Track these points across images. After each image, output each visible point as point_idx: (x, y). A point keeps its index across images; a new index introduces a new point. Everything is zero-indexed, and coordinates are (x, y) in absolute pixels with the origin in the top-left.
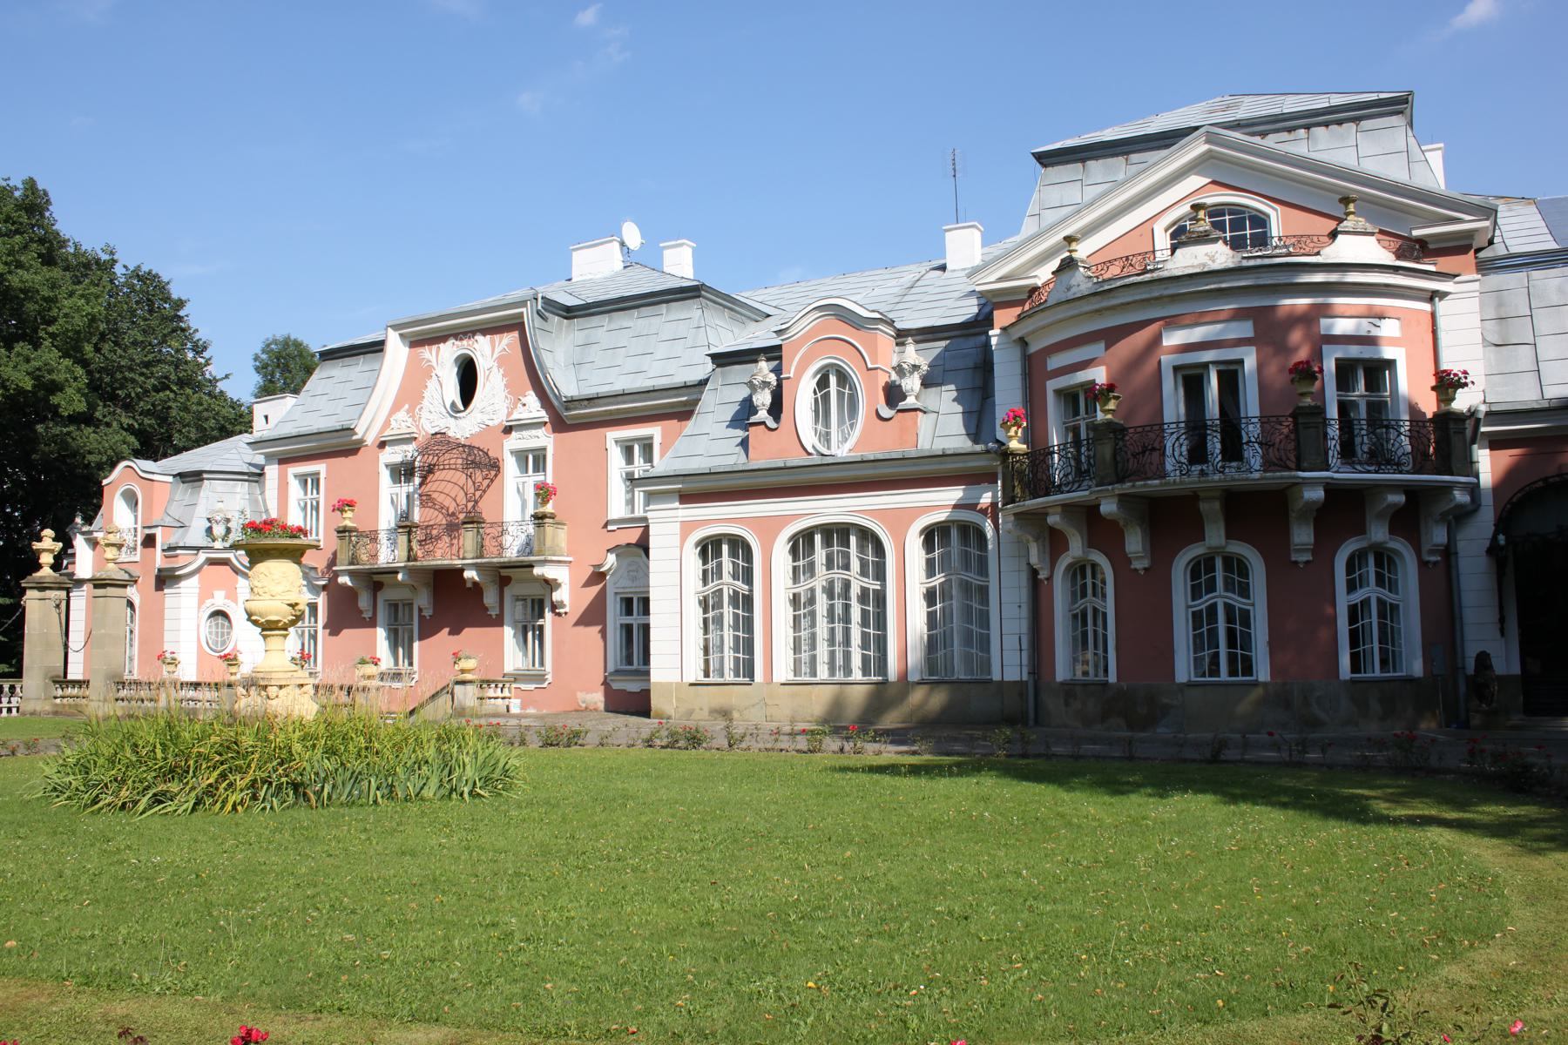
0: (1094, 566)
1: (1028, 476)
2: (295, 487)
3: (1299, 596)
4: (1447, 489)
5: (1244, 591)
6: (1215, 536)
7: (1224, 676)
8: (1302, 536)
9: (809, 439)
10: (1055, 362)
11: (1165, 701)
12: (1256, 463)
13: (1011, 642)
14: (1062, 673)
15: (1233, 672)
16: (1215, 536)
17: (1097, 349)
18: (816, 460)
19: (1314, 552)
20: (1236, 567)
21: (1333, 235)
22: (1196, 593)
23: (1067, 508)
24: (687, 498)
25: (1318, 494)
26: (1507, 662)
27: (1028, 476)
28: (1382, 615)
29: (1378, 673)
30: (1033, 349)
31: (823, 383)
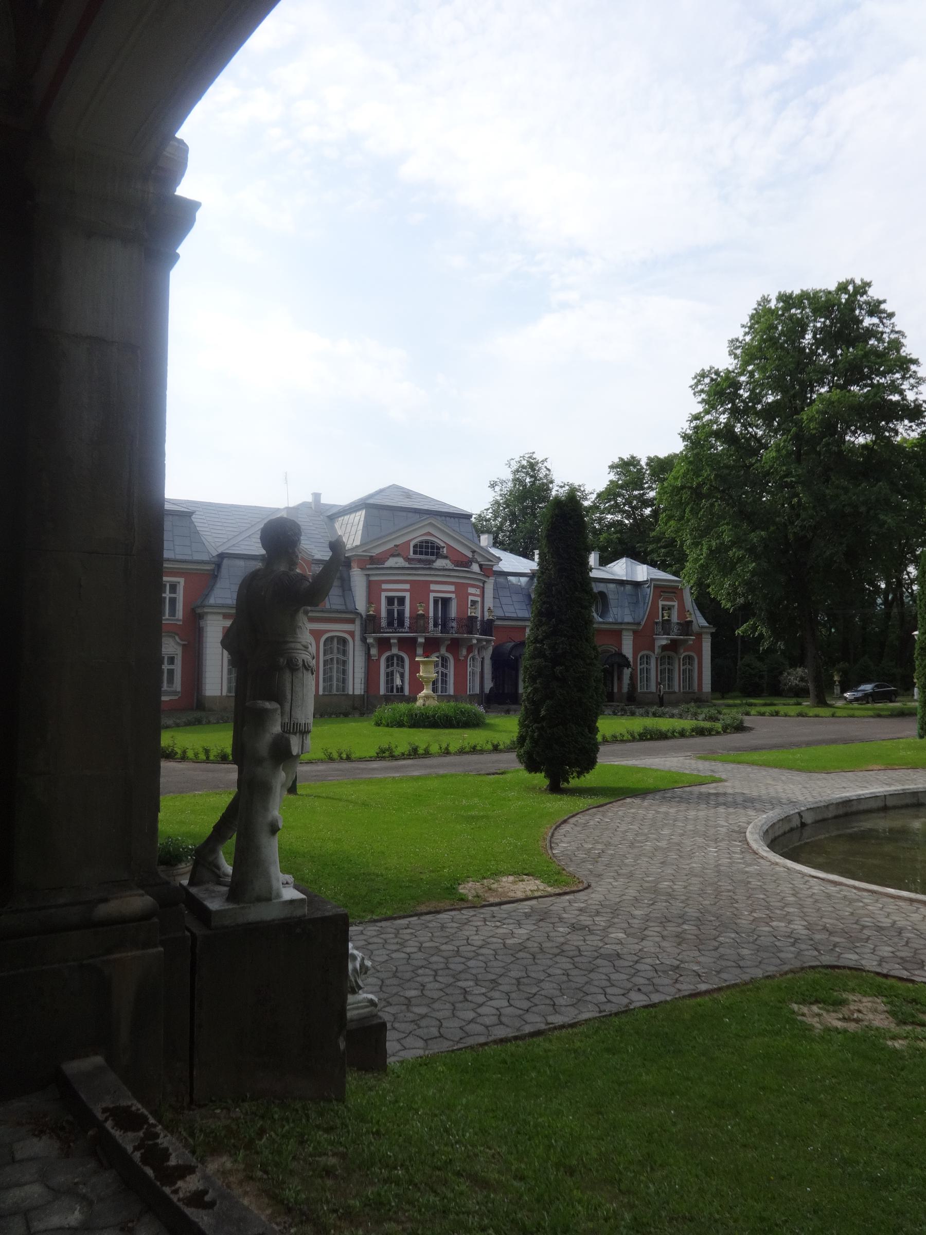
5: (446, 668)
6: (443, 651)
10: (384, 586)
13: (357, 681)
17: (407, 586)
27: (370, 623)
30: (372, 578)
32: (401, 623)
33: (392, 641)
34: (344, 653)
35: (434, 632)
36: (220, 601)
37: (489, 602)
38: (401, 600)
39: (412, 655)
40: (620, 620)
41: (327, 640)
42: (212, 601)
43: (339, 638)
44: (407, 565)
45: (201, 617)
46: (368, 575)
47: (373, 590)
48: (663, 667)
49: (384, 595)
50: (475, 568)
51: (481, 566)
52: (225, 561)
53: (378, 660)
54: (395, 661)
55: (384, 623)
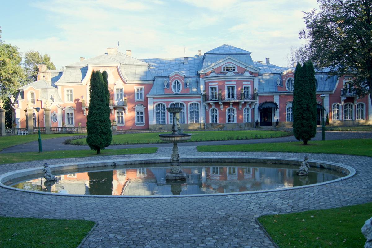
0: (215, 109)
1: (206, 98)
2: (66, 93)
3: (240, 112)
4: (255, 102)
5: (234, 113)
6: (231, 107)
7: (231, 122)
8: (240, 107)
9: (173, 91)
10: (209, 84)
11: (225, 125)
12: (236, 99)
14: (210, 122)
15: (232, 122)
16: (231, 107)
18: (175, 94)
19: (241, 109)
20: (233, 110)
21: (245, 71)
22: (228, 113)
23: (213, 103)
24: (154, 98)
25: (243, 103)
26: (259, 121)
28: (247, 116)
29: (247, 122)
30: (206, 81)
31: (175, 83)
32: (216, 98)
33: (211, 104)
34: (198, 109)
35: (227, 100)
36: (152, 93)
37: (256, 86)
38: (215, 88)
39: (220, 109)
40: (322, 90)
41: (191, 105)
42: (150, 93)
43: (195, 104)
44: (217, 76)
45: (148, 98)
46: (205, 80)
47: (206, 85)
48: (358, 109)
49: (210, 87)
50: (247, 74)
51: (252, 73)
52: (156, 79)
53: (209, 111)
54: (214, 111)
55: (210, 98)
